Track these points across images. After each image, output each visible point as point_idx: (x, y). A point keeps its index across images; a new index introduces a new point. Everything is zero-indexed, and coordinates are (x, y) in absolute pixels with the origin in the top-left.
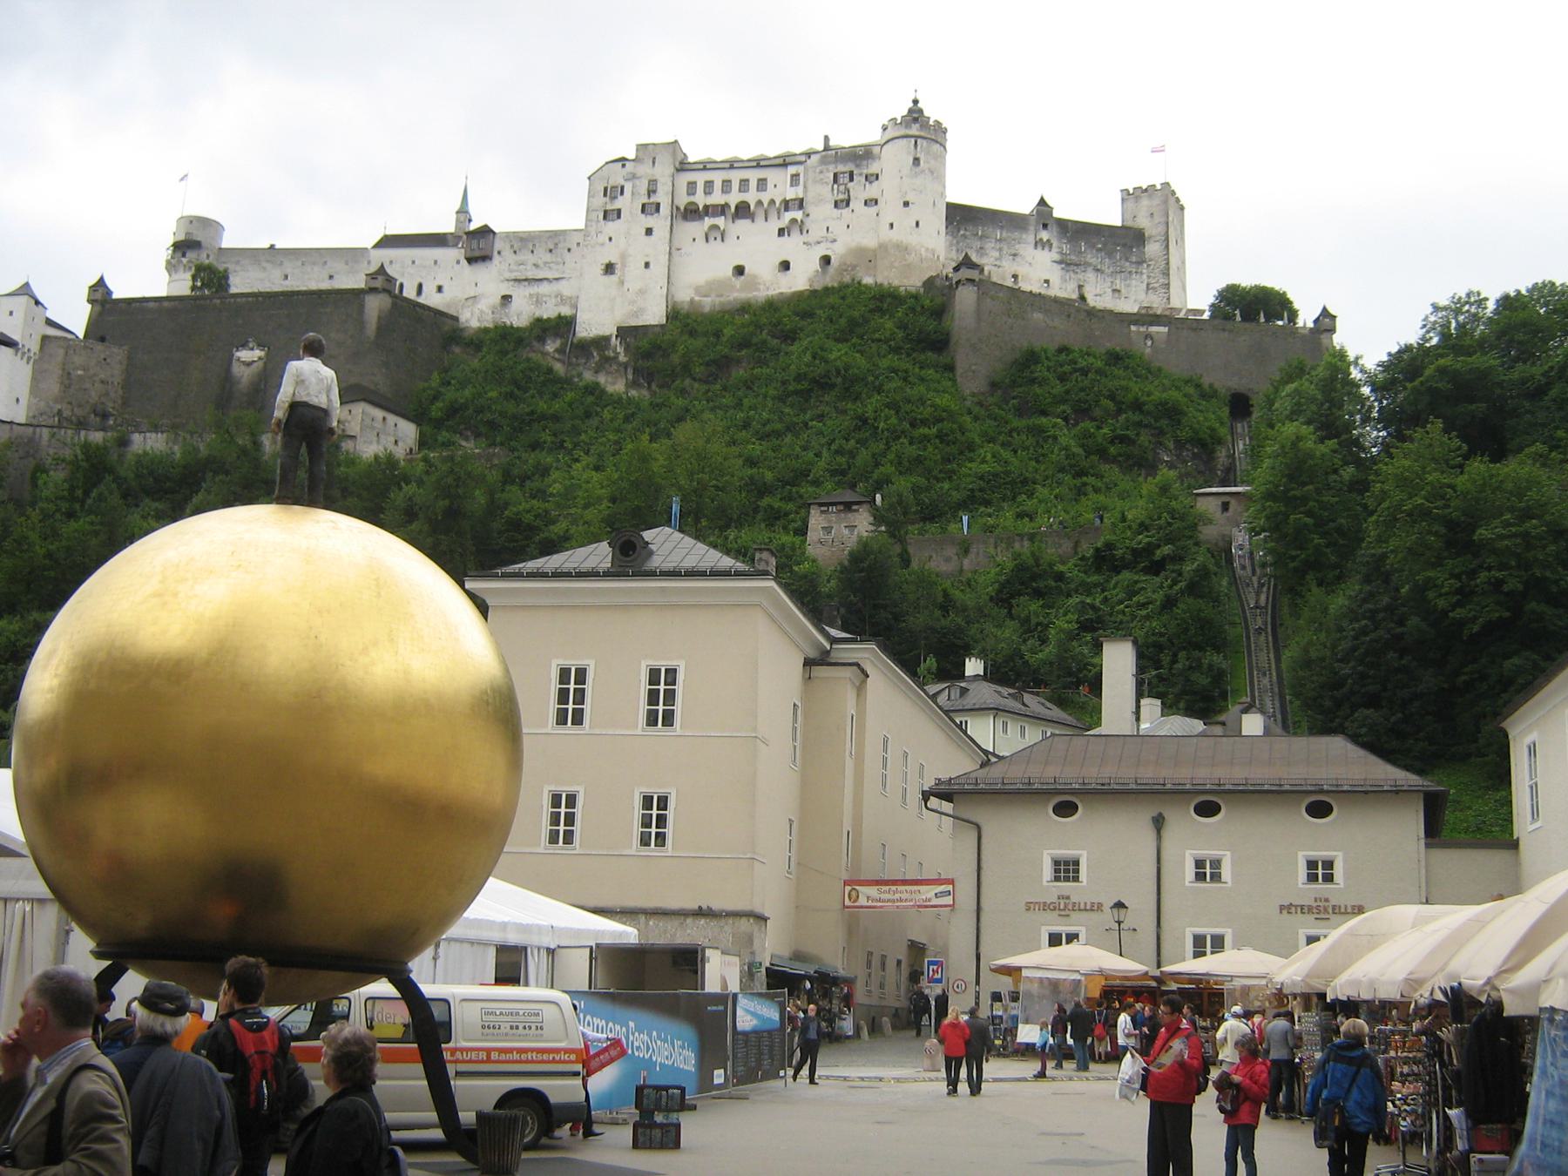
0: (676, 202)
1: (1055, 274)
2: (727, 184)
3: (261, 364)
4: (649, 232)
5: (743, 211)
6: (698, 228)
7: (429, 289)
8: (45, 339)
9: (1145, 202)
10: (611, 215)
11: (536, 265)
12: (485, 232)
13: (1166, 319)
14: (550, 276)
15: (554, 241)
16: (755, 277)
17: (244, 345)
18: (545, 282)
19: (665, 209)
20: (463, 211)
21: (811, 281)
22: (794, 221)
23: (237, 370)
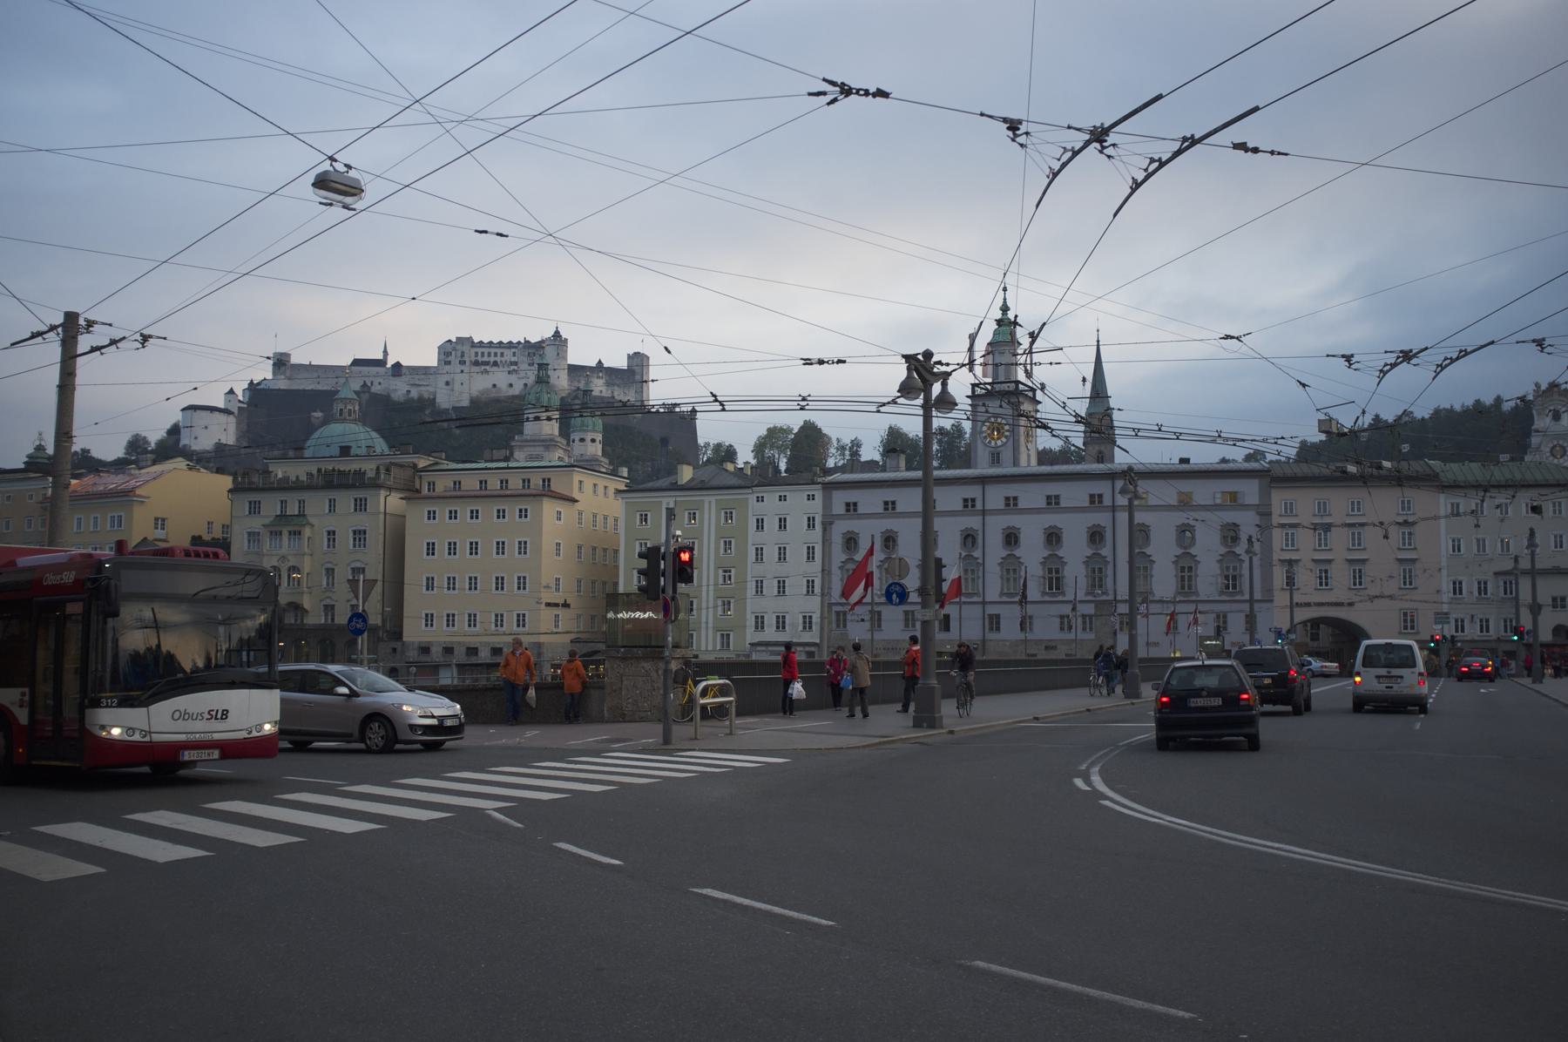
1: (604, 389)
2: (489, 354)
5: (495, 364)
6: (476, 369)
7: (376, 383)
8: (239, 408)
10: (449, 363)
12: (398, 365)
13: (642, 408)
15: (425, 370)
16: (499, 388)
17: (315, 411)
20: (385, 352)
21: (520, 392)
22: (514, 370)
23: (313, 419)
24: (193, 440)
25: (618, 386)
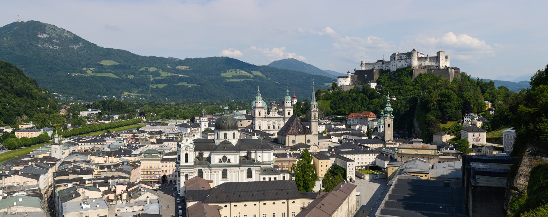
5: (402, 59)
10: (392, 60)
15: (389, 62)
17: (365, 75)
20: (383, 58)
25: (433, 61)
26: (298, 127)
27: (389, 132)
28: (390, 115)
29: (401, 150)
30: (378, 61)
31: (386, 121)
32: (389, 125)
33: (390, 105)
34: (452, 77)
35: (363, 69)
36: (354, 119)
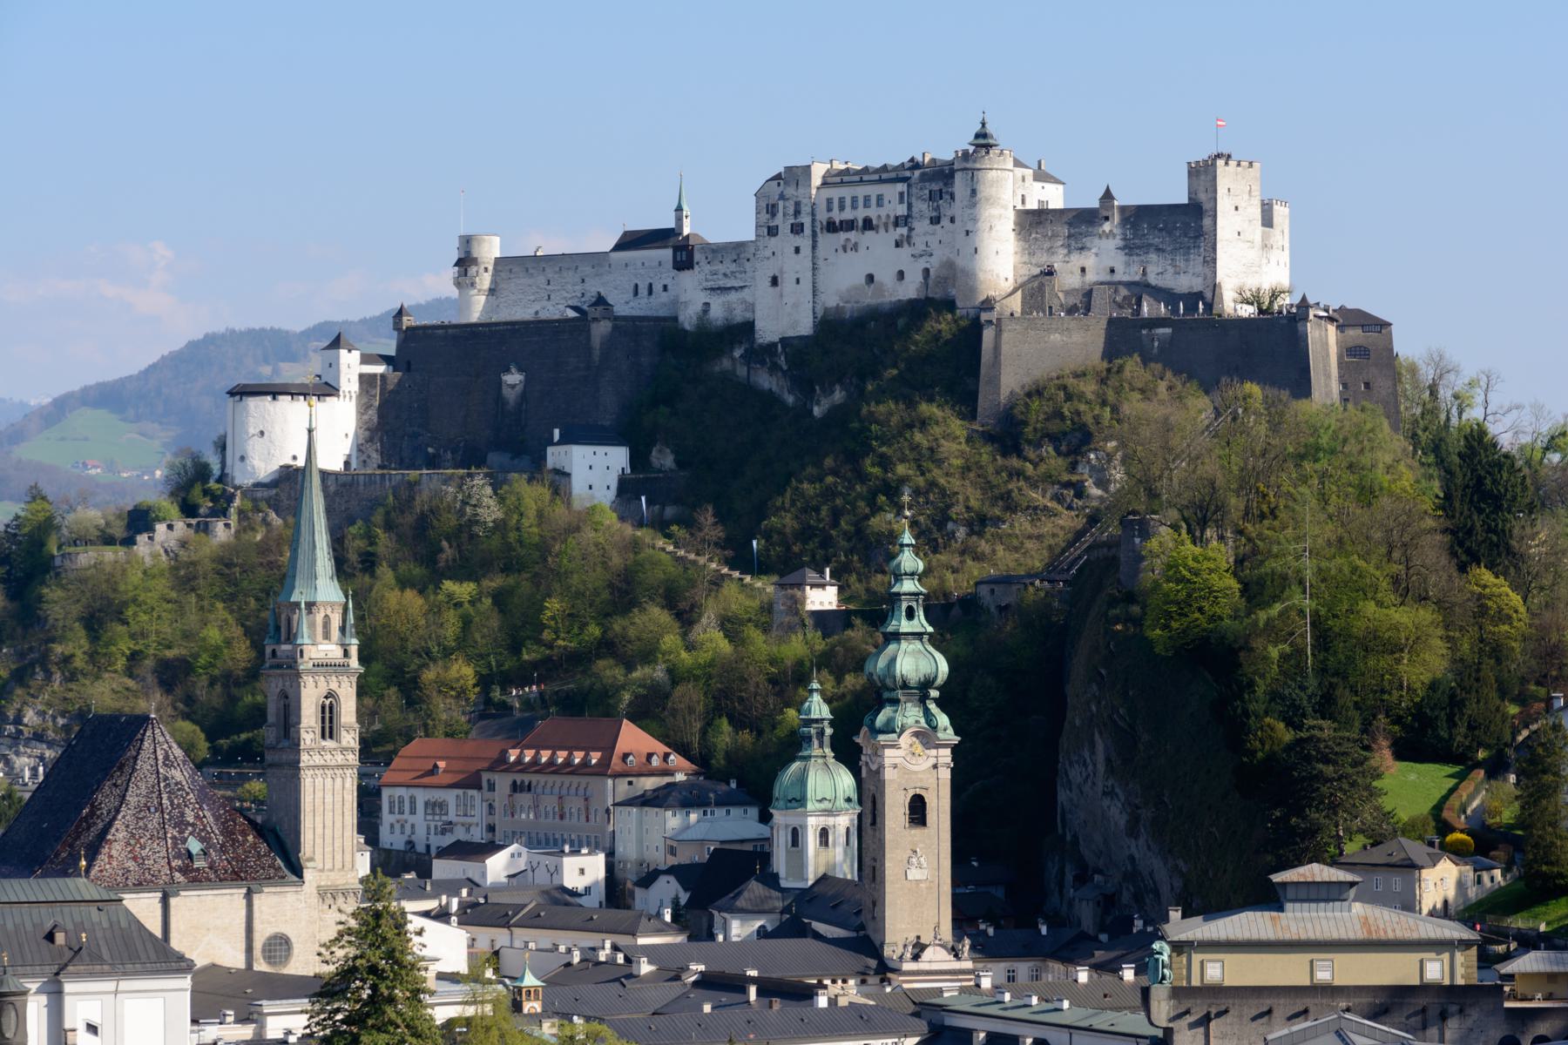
0: (818, 217)
1: (1118, 260)
3: (522, 386)
4: (797, 250)
5: (868, 225)
7: (658, 287)
8: (361, 376)
9: (1203, 177)
10: (773, 231)
11: (725, 275)
14: (736, 285)
15: (736, 251)
17: (508, 371)
18: (733, 292)
19: (807, 230)
20: (679, 209)
23: (506, 392)
24: (238, 463)
25: (1159, 250)
26: (181, 824)
27: (914, 874)
28: (927, 712)
29: (1197, 958)
30: (632, 241)
31: (889, 774)
32: (918, 811)
33: (920, 623)
34: (1329, 393)
35: (477, 309)
36: (450, 796)
